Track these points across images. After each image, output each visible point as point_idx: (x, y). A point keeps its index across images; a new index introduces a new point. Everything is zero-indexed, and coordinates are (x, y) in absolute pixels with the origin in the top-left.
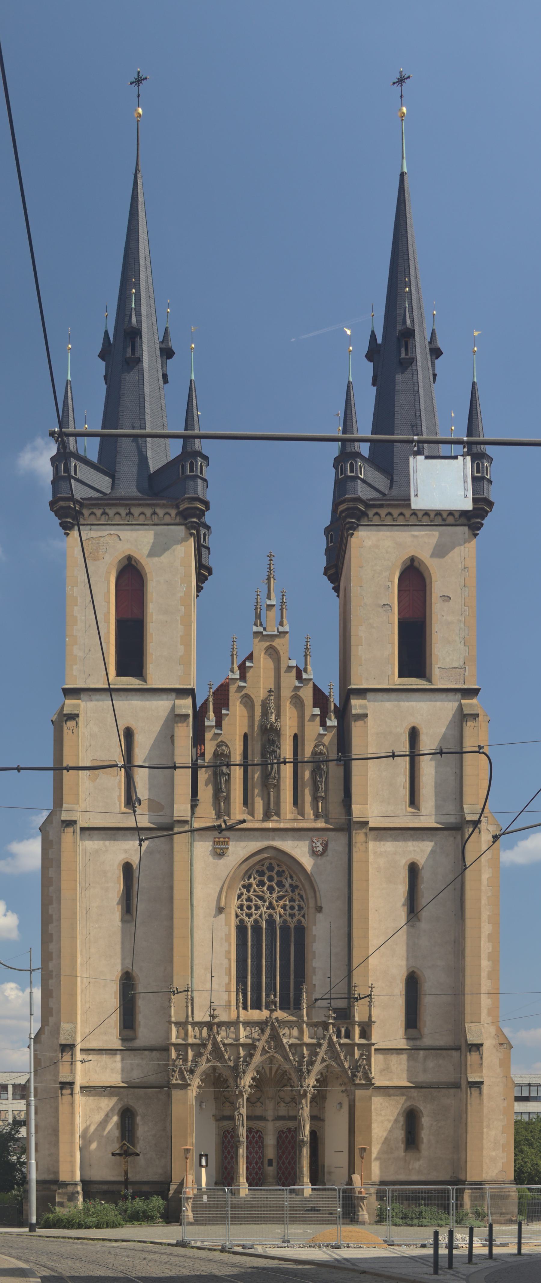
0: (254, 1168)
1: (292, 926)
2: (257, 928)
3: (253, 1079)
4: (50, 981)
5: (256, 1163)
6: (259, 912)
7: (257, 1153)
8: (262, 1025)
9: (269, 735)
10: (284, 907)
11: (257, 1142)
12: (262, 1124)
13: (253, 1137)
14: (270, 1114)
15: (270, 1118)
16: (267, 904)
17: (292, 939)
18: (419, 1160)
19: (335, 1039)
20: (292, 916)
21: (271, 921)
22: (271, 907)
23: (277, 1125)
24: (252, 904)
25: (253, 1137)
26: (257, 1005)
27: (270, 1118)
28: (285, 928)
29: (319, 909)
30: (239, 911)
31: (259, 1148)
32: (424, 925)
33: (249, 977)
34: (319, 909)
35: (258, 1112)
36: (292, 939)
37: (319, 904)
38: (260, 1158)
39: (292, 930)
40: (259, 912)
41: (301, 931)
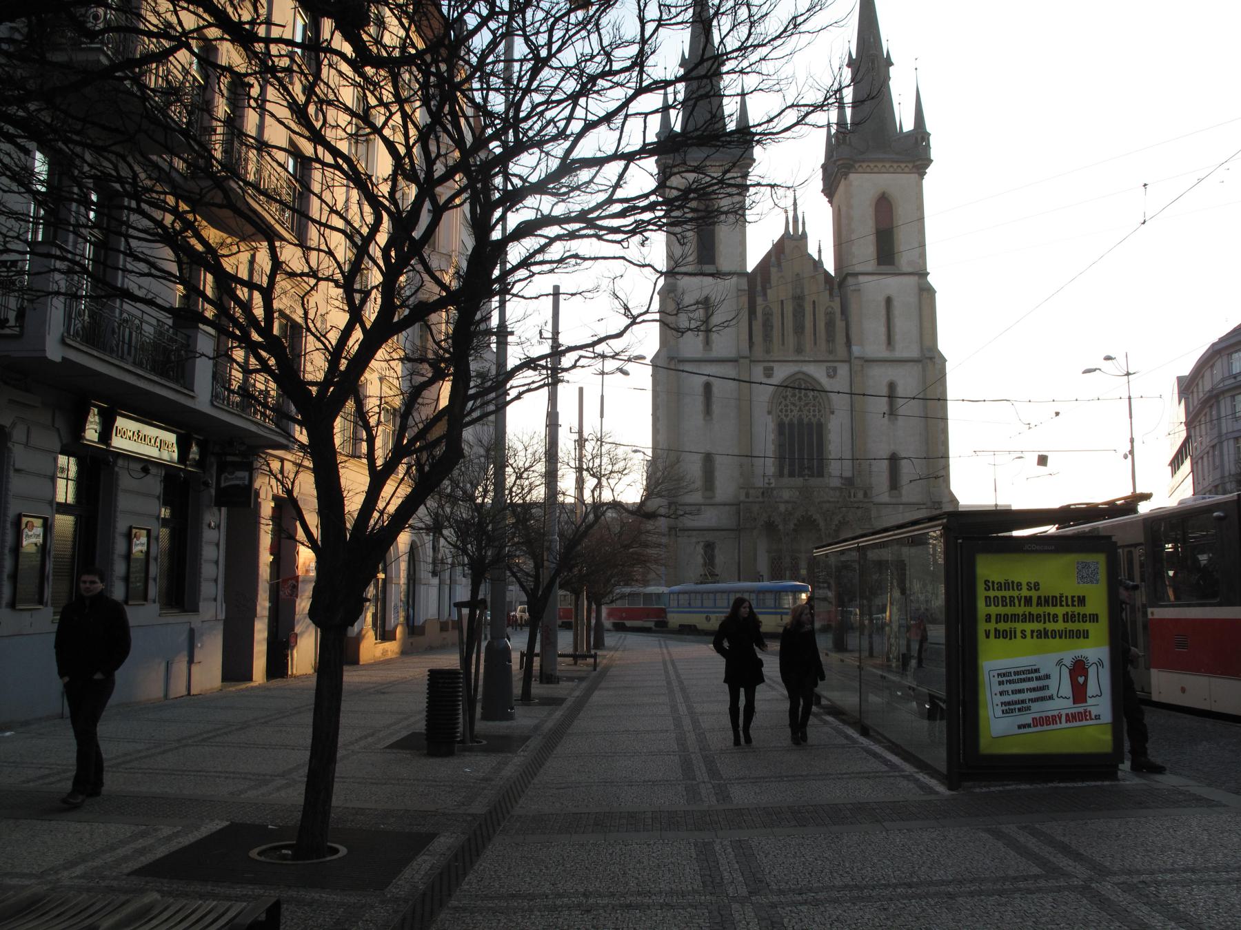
2: (791, 425)
9: (799, 299)
22: (800, 410)
26: (792, 475)
28: (810, 424)
34: (833, 413)
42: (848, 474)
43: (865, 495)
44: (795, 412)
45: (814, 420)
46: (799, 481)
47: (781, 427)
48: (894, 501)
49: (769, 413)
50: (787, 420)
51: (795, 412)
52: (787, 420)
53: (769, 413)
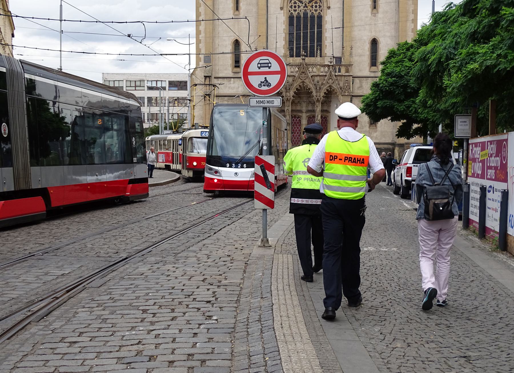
0: (296, 136)
1: (316, 16)
2: (299, 17)
3: (295, 93)
4: (200, 45)
5: (298, 133)
6: (300, 9)
7: (298, 128)
8: (299, 66)
10: (312, 6)
11: (298, 123)
12: (300, 114)
13: (296, 120)
14: (304, 109)
15: (304, 111)
16: (304, 5)
17: (316, 22)
18: (376, 132)
19: (333, 73)
20: (316, 11)
21: (305, 14)
22: (306, 6)
23: (308, 114)
24: (297, 5)
25: (296, 120)
26: (298, 55)
27: (304, 111)
28: (312, 17)
29: (329, 8)
30: (290, 9)
31: (299, 126)
32: (380, 15)
33: (295, 42)
34: (329, 8)
35: (298, 108)
36: (316, 22)
37: (329, 6)
38: (299, 130)
39: (316, 18)
40: (300, 9)
41: (320, 18)
42: (337, 54)
43: (347, 71)
44: (302, 8)
45: (316, 14)
46: (298, 60)
47: (291, 18)
48: (372, 75)
49: (282, 8)
50: (295, 14)
51: (302, 8)
52: (295, 14)
53: (282, 8)
